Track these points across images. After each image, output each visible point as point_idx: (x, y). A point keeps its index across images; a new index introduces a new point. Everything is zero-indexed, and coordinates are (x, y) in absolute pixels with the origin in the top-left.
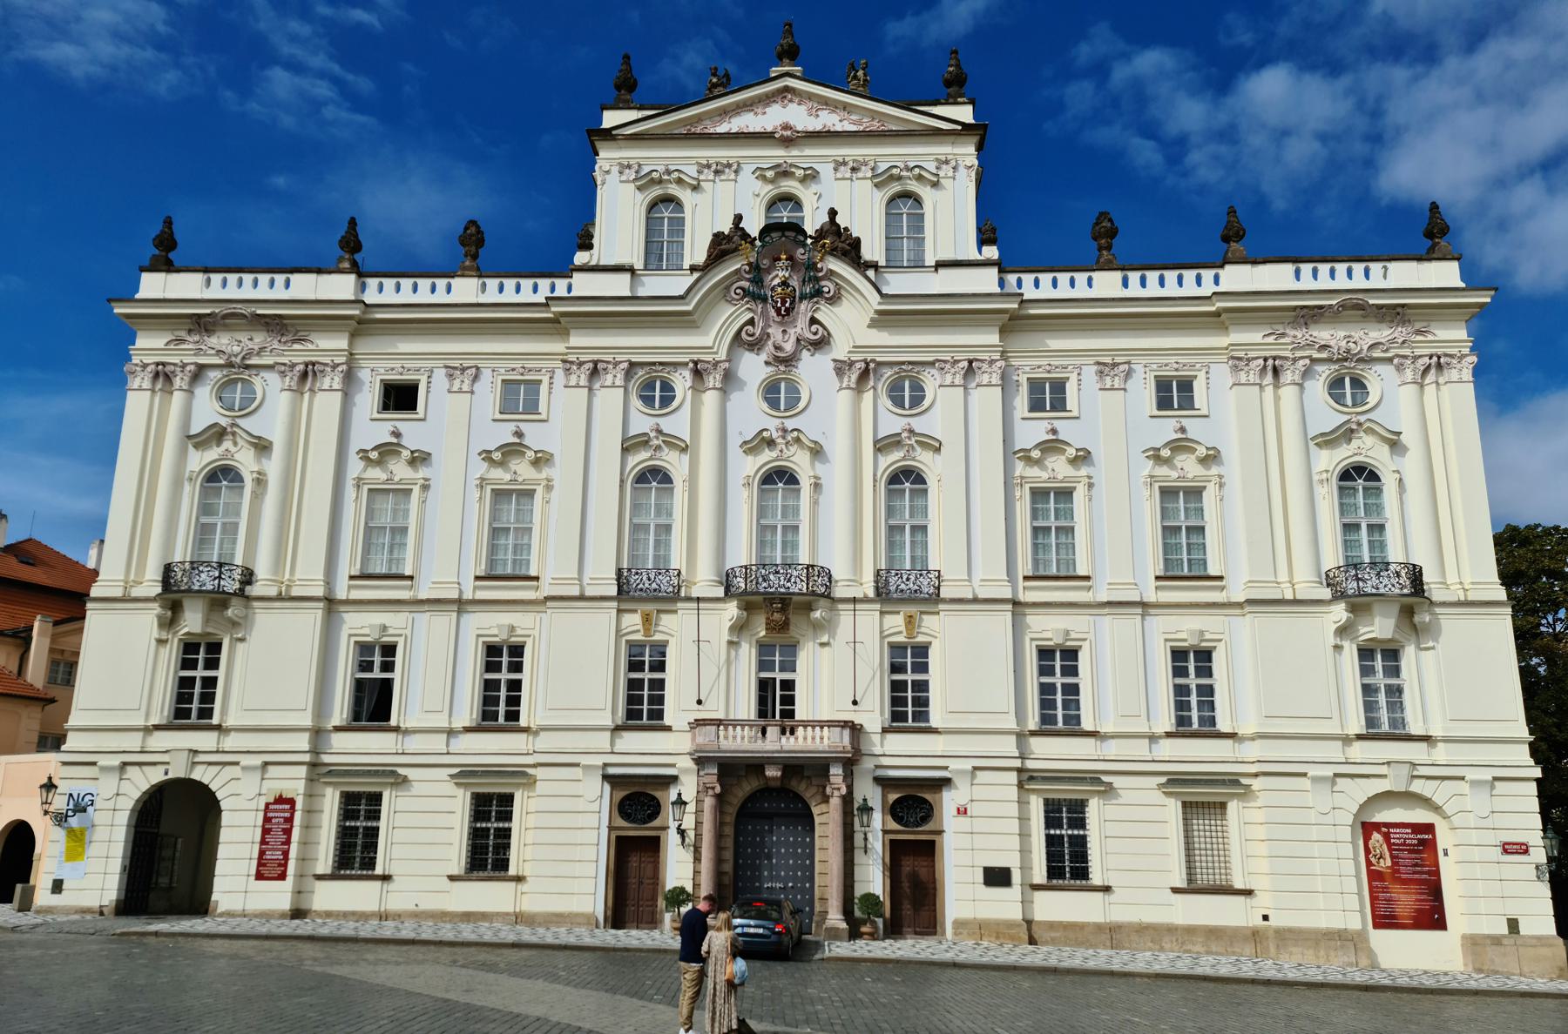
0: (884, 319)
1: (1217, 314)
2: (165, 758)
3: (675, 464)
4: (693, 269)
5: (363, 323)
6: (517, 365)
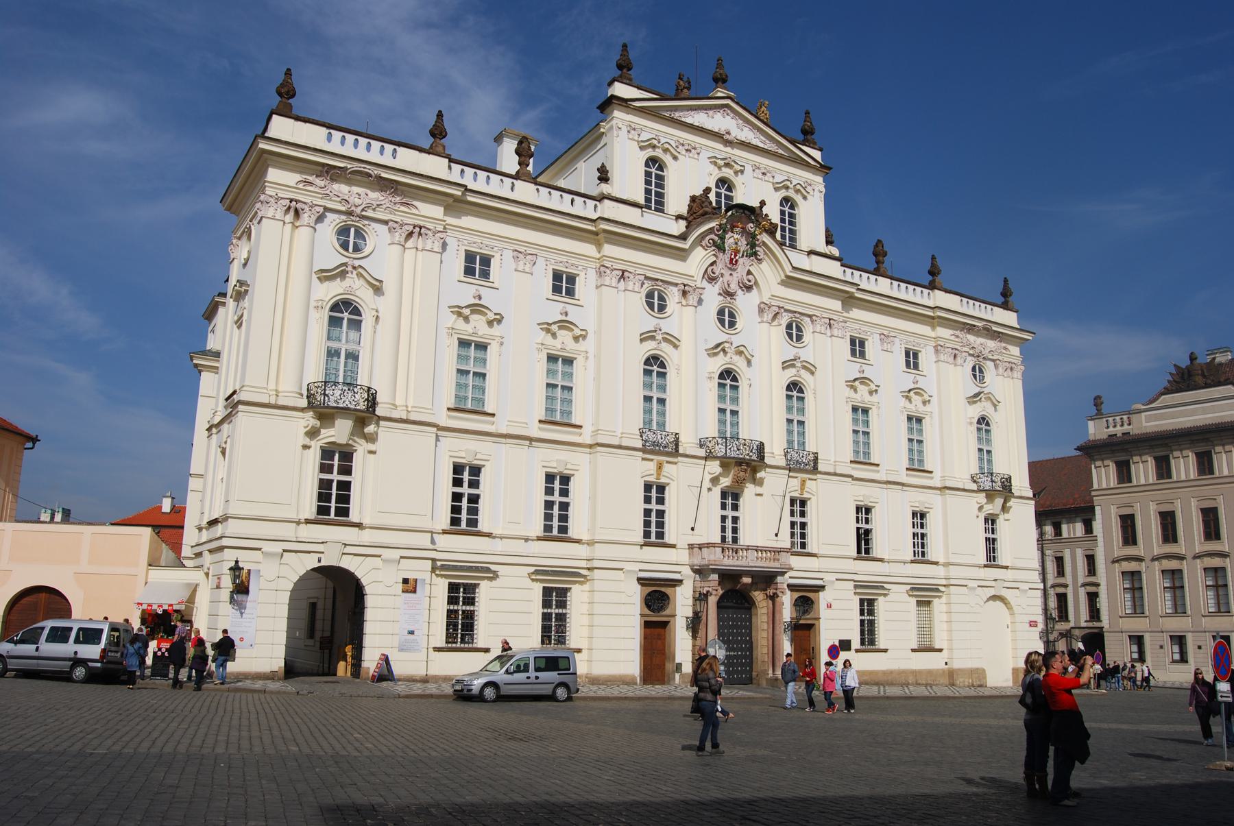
0: (789, 282)
1: (933, 318)
2: (320, 548)
4: (679, 217)
5: (458, 203)
6: (564, 259)
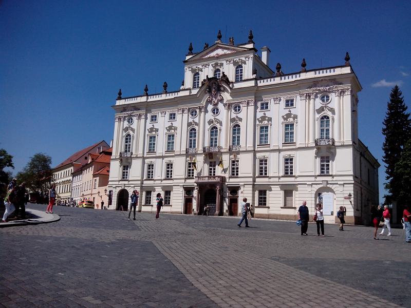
3: (196, 128)
5: (148, 107)
